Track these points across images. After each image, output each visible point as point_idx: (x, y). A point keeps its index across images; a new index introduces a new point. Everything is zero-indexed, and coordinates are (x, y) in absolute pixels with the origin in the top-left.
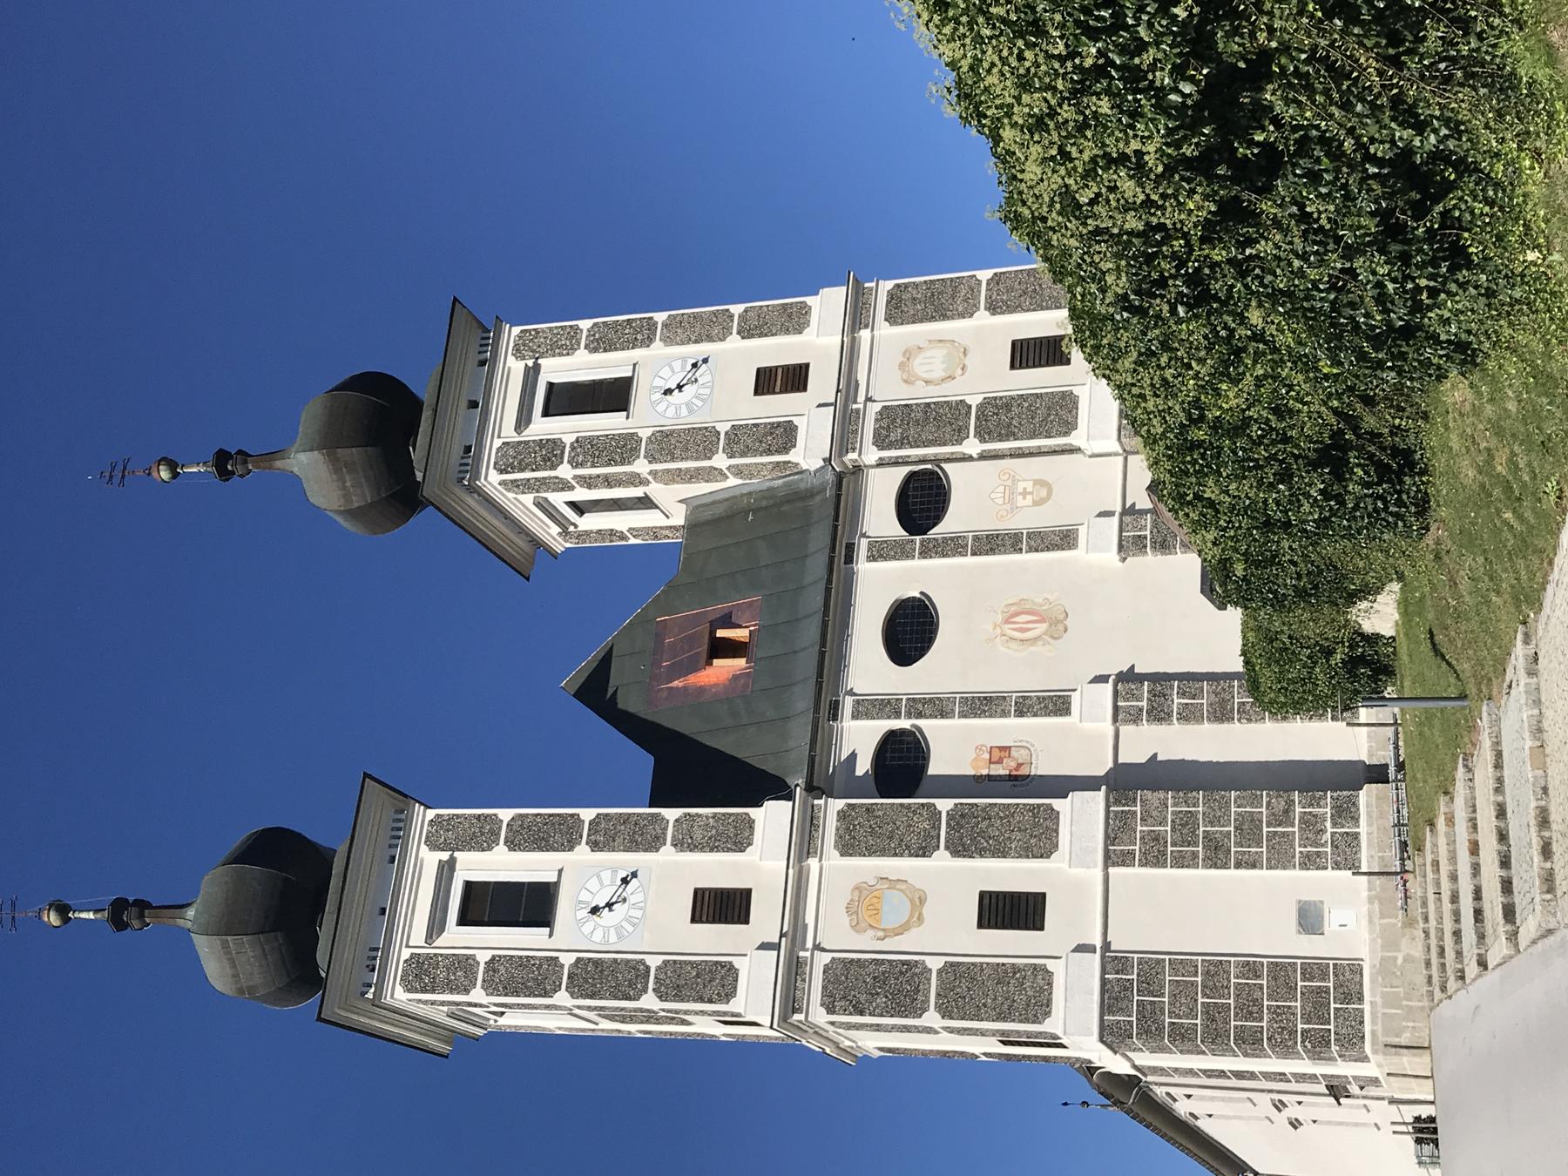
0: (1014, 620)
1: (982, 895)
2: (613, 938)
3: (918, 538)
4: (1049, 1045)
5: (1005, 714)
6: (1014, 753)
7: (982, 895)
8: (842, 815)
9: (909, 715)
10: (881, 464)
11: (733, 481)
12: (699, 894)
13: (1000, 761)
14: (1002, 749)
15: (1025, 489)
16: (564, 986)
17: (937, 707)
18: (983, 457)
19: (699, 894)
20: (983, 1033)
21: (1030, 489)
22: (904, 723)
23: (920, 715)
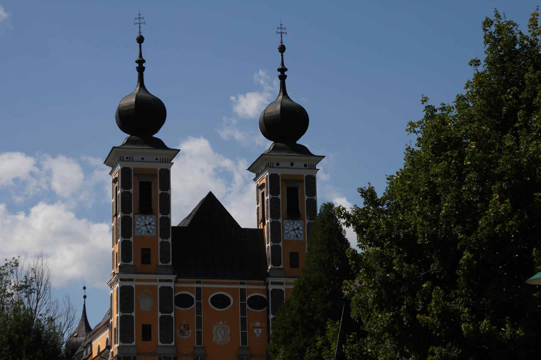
0: (223, 330)
1: (150, 325)
2: (137, 227)
3: (246, 302)
4: (115, 342)
5: (197, 328)
6: (187, 331)
7: (150, 325)
8: (170, 288)
9: (197, 303)
10: (268, 291)
11: (267, 246)
12: (148, 250)
13: (185, 327)
14: (188, 328)
15: (259, 331)
16: (124, 215)
17: (199, 311)
18: (268, 319)
19: (148, 250)
20: (117, 325)
21: (259, 332)
22: (195, 301)
23: (196, 305)
